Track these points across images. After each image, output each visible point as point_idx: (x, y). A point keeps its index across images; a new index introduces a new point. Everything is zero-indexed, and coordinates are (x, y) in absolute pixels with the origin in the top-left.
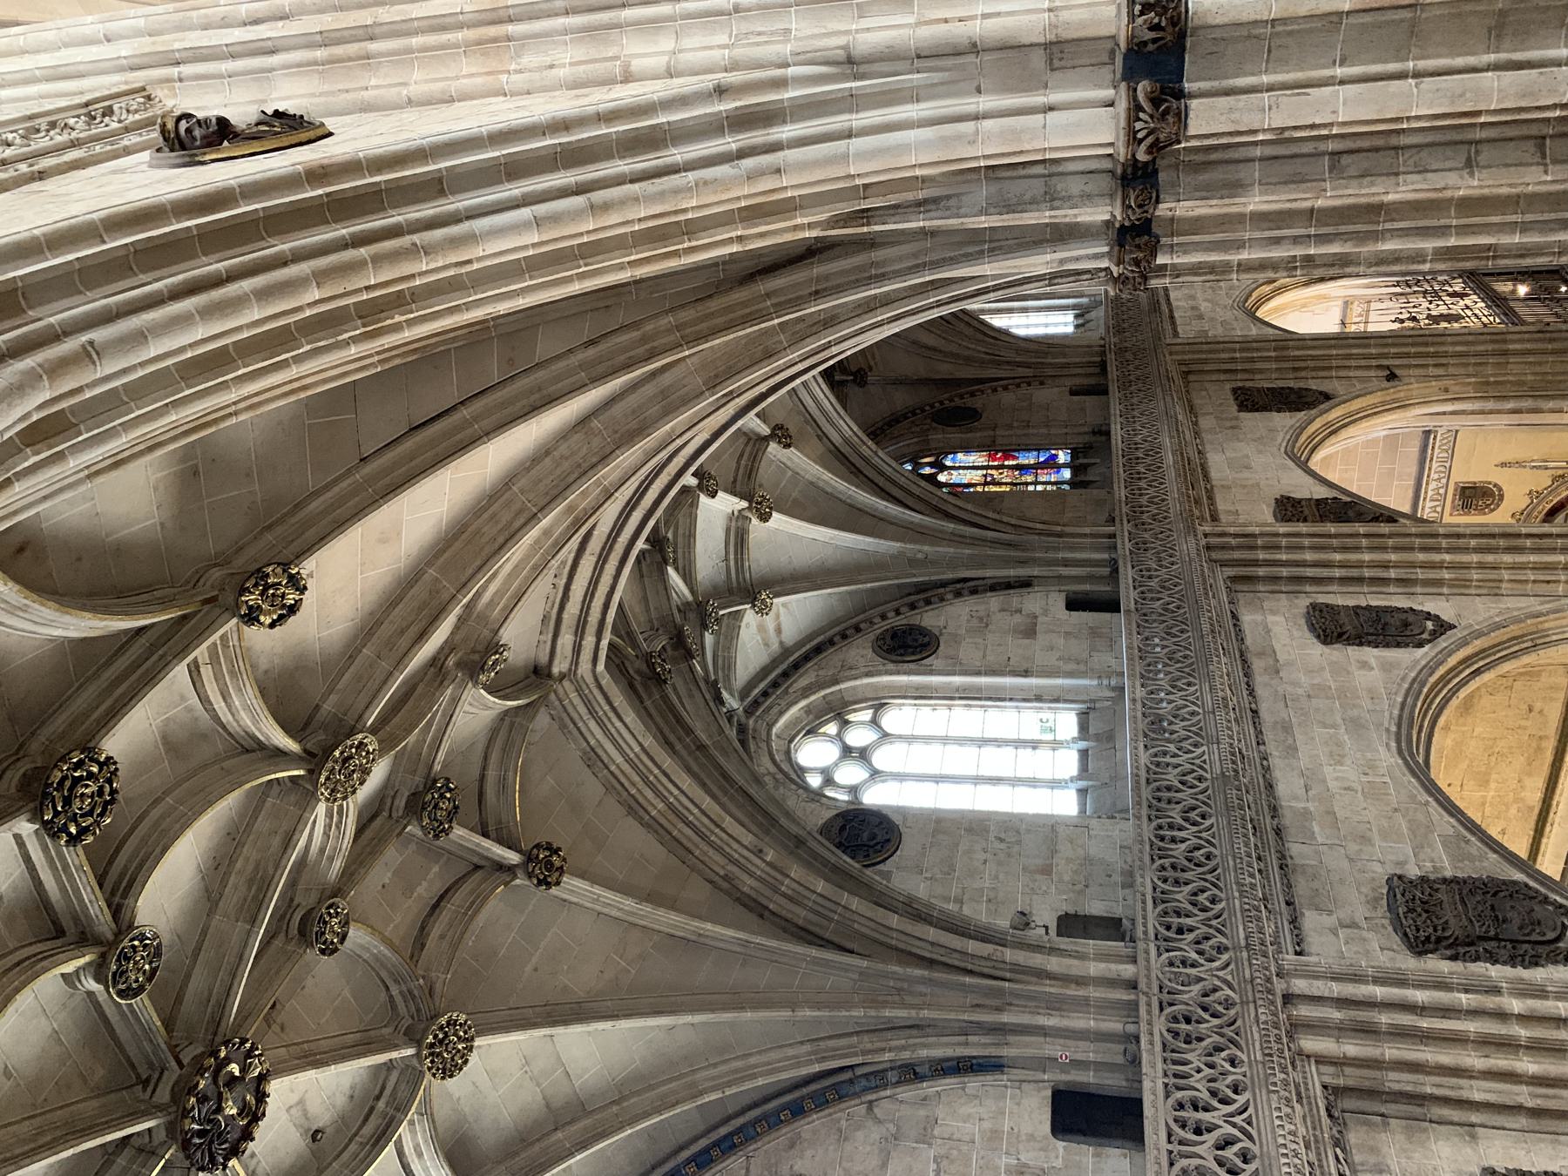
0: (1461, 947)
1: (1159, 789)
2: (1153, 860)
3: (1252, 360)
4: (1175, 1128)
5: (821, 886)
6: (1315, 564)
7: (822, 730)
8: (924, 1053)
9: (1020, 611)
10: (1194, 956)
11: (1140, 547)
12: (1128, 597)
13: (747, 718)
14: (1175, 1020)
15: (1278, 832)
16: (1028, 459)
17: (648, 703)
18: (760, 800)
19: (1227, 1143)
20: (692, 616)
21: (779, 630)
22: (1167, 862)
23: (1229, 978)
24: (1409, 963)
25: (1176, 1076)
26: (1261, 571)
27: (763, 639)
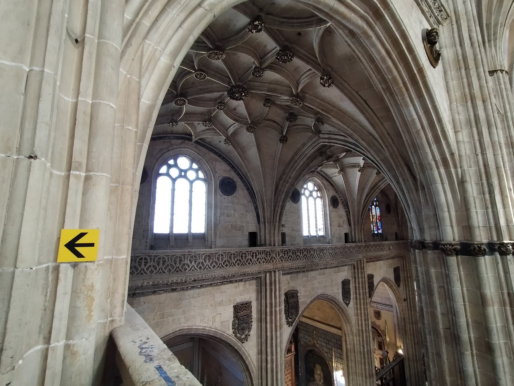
0: (287, 301)
1: (310, 250)
3: (407, 271)
4: (252, 252)
5: (285, 190)
6: (359, 282)
8: (259, 210)
9: (344, 224)
10: (280, 256)
11: (360, 247)
12: (348, 245)
15: (304, 271)
16: (379, 224)
18: (299, 177)
19: (251, 261)
20: (336, 158)
21: (335, 176)
22: (296, 251)
24: (283, 292)
26: (356, 271)
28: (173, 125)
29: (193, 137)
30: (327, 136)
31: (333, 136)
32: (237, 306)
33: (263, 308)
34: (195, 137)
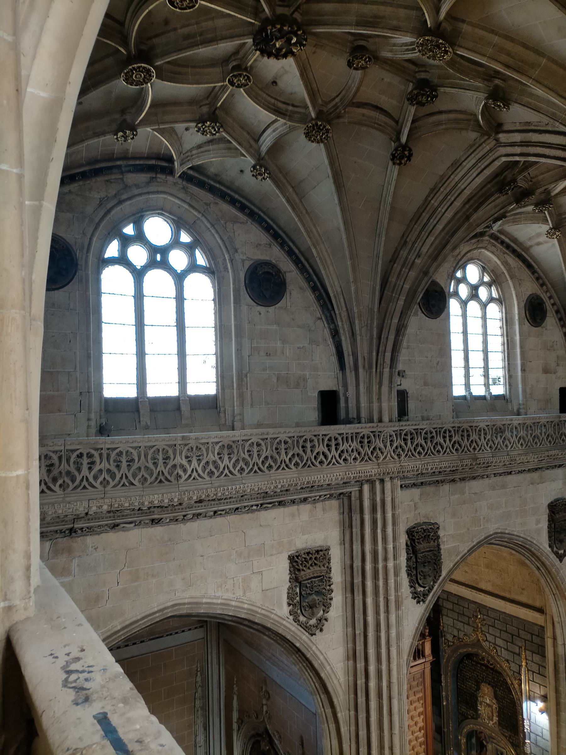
0: (412, 548)
1: (468, 431)
2: (434, 429)
4: (328, 437)
5: (407, 286)
7: (485, 274)
10: (395, 445)
13: (489, 236)
14: (368, 437)
15: (453, 481)
17: (489, 186)
18: (444, 251)
19: (326, 457)
20: (543, 196)
21: (539, 244)
23: (388, 458)
24: (402, 528)
25: (347, 438)
27: (533, 237)
28: (125, 137)
29: (176, 163)
30: (517, 137)
31: (535, 137)
32: (297, 557)
33: (357, 563)
34: (181, 165)
